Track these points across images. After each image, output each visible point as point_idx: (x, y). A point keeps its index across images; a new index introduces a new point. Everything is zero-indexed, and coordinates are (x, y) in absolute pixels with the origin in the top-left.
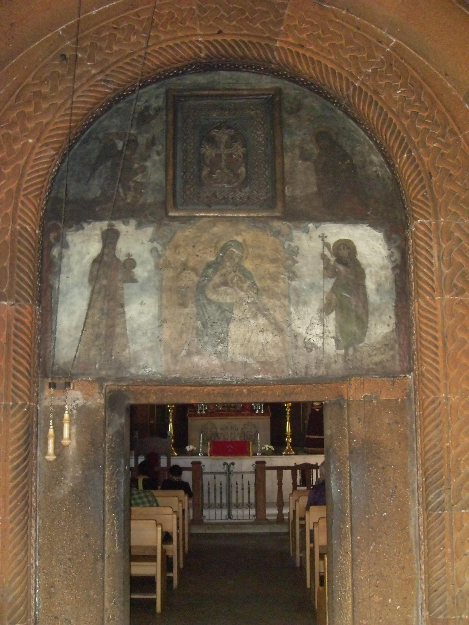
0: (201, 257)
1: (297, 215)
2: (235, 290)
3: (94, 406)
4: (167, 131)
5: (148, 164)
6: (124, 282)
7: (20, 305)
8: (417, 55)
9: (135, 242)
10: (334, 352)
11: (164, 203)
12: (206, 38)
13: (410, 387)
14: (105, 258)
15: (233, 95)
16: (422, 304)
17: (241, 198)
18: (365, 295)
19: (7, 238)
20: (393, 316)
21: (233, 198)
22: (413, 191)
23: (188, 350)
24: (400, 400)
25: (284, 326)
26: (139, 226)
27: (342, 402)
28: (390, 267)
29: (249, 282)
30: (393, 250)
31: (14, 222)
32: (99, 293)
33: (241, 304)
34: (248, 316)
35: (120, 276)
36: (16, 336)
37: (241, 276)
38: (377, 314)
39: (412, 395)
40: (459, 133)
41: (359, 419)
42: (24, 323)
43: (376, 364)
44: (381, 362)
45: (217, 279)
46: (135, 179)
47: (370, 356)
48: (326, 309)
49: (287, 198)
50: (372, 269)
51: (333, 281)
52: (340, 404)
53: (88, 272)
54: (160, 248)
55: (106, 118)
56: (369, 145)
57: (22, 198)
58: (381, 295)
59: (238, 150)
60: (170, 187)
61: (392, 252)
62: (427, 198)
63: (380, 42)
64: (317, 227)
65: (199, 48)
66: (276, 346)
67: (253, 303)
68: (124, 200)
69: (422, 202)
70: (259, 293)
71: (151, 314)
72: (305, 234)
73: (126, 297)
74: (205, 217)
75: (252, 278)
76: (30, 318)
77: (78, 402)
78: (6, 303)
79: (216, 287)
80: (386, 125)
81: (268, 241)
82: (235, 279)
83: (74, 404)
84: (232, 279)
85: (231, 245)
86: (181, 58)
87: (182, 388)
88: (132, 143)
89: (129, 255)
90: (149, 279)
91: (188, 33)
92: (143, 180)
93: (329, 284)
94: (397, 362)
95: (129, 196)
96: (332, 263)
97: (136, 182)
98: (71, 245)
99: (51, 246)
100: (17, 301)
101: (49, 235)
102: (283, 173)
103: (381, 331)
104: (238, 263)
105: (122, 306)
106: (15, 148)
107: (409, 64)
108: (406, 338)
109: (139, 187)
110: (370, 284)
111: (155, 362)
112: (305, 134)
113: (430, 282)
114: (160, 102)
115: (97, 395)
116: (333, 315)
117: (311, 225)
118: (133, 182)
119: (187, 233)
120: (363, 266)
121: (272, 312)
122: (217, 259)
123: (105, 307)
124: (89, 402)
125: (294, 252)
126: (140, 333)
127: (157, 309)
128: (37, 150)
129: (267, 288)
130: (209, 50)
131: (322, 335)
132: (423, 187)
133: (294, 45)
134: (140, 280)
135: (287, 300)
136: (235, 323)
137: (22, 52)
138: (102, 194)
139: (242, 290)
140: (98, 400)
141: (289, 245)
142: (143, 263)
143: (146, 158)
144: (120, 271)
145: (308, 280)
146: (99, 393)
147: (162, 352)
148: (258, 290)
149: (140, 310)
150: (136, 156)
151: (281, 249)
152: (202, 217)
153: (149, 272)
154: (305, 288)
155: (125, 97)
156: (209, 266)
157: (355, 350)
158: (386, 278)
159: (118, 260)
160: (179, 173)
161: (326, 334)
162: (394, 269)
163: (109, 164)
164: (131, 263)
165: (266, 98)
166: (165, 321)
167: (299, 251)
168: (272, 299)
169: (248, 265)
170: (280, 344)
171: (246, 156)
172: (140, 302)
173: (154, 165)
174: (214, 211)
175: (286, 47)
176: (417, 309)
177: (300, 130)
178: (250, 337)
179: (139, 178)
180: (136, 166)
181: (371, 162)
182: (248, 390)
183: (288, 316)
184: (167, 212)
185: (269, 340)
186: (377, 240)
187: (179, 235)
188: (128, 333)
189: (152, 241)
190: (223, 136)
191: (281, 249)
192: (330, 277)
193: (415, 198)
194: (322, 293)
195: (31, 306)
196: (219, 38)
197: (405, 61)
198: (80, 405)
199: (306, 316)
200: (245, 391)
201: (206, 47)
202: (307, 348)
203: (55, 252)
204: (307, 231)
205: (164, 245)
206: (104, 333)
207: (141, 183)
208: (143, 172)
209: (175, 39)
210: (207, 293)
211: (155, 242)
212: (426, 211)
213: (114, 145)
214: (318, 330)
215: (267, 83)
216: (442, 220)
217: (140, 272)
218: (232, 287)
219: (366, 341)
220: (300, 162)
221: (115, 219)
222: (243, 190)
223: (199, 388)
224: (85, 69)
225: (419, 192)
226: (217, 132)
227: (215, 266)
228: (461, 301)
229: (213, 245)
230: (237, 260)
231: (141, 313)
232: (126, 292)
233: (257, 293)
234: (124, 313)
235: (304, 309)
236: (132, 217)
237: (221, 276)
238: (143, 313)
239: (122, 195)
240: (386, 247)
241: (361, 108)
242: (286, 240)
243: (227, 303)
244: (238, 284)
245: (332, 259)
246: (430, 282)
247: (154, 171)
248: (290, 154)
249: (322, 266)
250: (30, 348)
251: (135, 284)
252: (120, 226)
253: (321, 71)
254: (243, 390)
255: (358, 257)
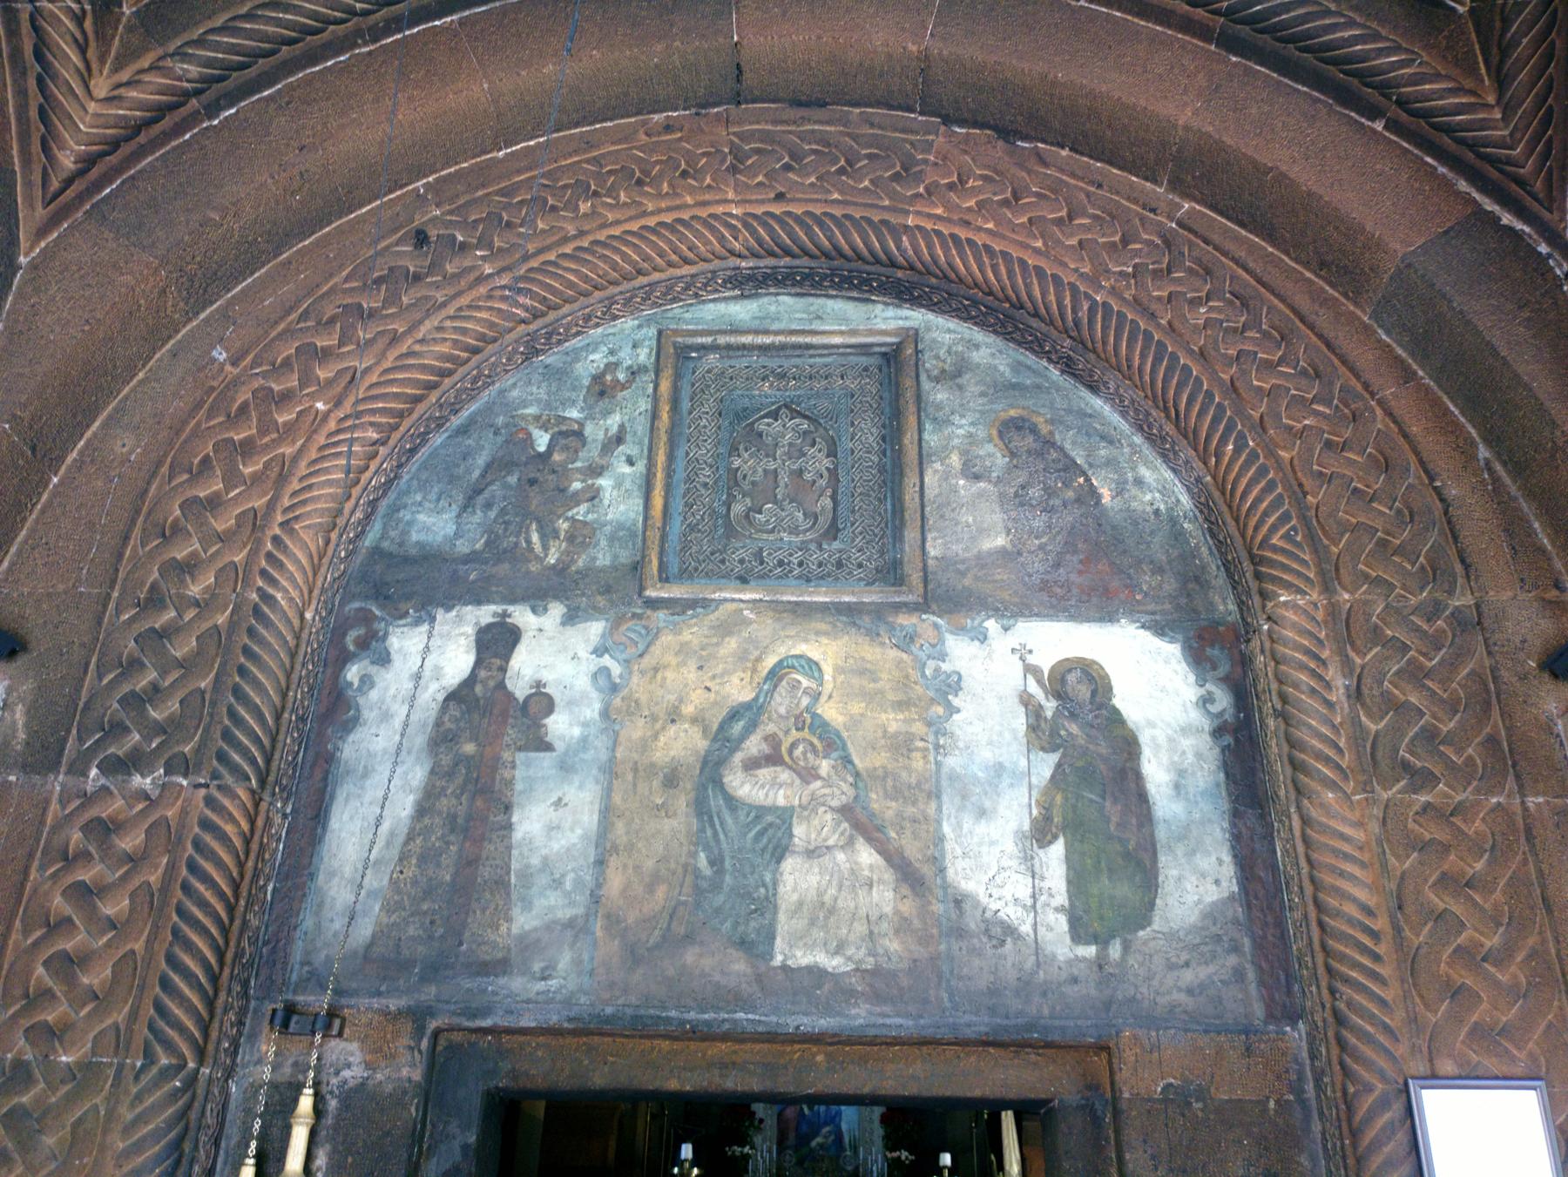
0: (717, 693)
1: (956, 598)
2: (799, 774)
3: (389, 1088)
4: (655, 415)
5: (604, 482)
6: (520, 749)
7: (219, 787)
8: (1243, 232)
9: (557, 656)
10: (1066, 950)
11: (637, 567)
12: (750, 209)
13: (1296, 1061)
14: (478, 689)
15: (808, 347)
16: (1314, 813)
17: (820, 565)
18: (1143, 797)
19: (221, 619)
20: (1227, 858)
21: (800, 564)
22: (1256, 528)
23: (669, 928)
24: (1272, 1104)
25: (927, 870)
26: (570, 619)
27: (1097, 1106)
28: (1207, 728)
29: (835, 755)
30: (1209, 686)
31: (247, 582)
32: (450, 775)
33: (815, 811)
34: (831, 842)
35: (511, 734)
36: (193, 867)
37: (815, 741)
38: (1180, 850)
39: (1310, 1087)
40: (1367, 396)
41: (1153, 1157)
42: (223, 838)
43: (1190, 991)
44: (1203, 987)
45: (754, 745)
46: (570, 514)
47: (1171, 967)
48: (1041, 833)
49: (930, 562)
50: (1157, 732)
51: (1053, 758)
52: (1093, 1111)
53: (431, 721)
54: (616, 670)
55: (514, 385)
56: (1131, 445)
57: (277, 531)
58: (1187, 800)
59: (817, 461)
60: (654, 536)
61: (1209, 693)
62: (1298, 545)
63: (1153, 210)
64: (1006, 629)
65: (735, 227)
66: (902, 926)
67: (845, 811)
68: (540, 560)
69: (1283, 551)
70: (860, 784)
71: (579, 832)
72: (976, 643)
73: (519, 786)
74: (733, 600)
75: (844, 747)
76: (245, 826)
77: (346, 1073)
78: (185, 783)
79: (752, 765)
80: (1175, 381)
81: (883, 656)
82: (801, 748)
83: (334, 1081)
84: (793, 746)
85: (793, 667)
86: (690, 249)
87: (648, 1043)
88: (570, 437)
89: (539, 684)
90: (584, 741)
91: (707, 197)
92: (590, 517)
93: (1045, 766)
94: (1253, 988)
95: (553, 550)
96: (1049, 714)
97: (573, 520)
98: (394, 656)
99: (345, 658)
100: (215, 776)
101: (345, 634)
102: (923, 507)
103: (1196, 898)
104: (807, 709)
105: (508, 808)
106: (280, 420)
107: (1225, 254)
108: (1270, 919)
109: (581, 536)
110: (1156, 772)
111: (577, 962)
112: (972, 424)
113: (1331, 753)
114: (644, 356)
115: (405, 1057)
116: (1058, 849)
117: (992, 625)
118: (567, 519)
119: (686, 636)
120: (1131, 725)
121: (893, 835)
122: (756, 699)
123: (462, 811)
124: (379, 1076)
125: (949, 686)
126: (543, 880)
127: (596, 817)
128: (332, 425)
129: (880, 772)
130: (753, 232)
131: (1029, 902)
132: (1286, 518)
133: (949, 220)
134: (560, 746)
135: (933, 805)
136: (799, 860)
137: (329, 224)
138: (487, 544)
139: (818, 777)
140: (411, 1071)
141: (937, 670)
142: (571, 703)
143: (596, 471)
144: (511, 720)
145: (987, 755)
146: (411, 1049)
147: (599, 933)
148: (857, 775)
149: (551, 821)
150: (579, 464)
151: (914, 675)
152: (725, 600)
153: (585, 725)
154: (980, 774)
155: (559, 342)
156: (734, 715)
157: (1126, 947)
158: (1199, 755)
159: (510, 696)
160: (678, 505)
161: (1043, 898)
162: (1217, 732)
163: (512, 479)
164: (542, 701)
165: (885, 354)
166: (615, 849)
167: (963, 684)
168: (895, 799)
169: (830, 712)
170: (917, 923)
171: (833, 473)
172: (554, 799)
173: (618, 485)
174: (752, 590)
175: (929, 226)
176: (1297, 833)
177: (963, 416)
178: (836, 899)
179: (580, 512)
180: (577, 485)
181: (1139, 482)
182: (829, 1056)
183: (936, 845)
184: (642, 589)
185: (888, 909)
186: (1167, 662)
187: (666, 639)
188: (513, 880)
189: (599, 651)
190: (785, 431)
191: (914, 675)
192: (1043, 749)
193: (1264, 543)
194: (1026, 790)
195: (253, 792)
196: (777, 209)
197: (1216, 248)
198: (352, 1083)
199: (984, 849)
200: (819, 1058)
201: (746, 225)
202: (990, 937)
203: (353, 673)
204: (983, 638)
205: (627, 662)
206: (448, 878)
207: (585, 523)
208: (593, 499)
209: (678, 208)
210: (725, 780)
211: (607, 656)
212: (1299, 574)
213: (529, 440)
214: (1021, 887)
215: (886, 319)
216: (1347, 596)
217: (559, 725)
218: (790, 768)
219: (1157, 924)
220: (961, 482)
221: (513, 601)
222: (825, 546)
223: (693, 1045)
224: (467, 263)
225: (1274, 528)
226: (769, 425)
227: (749, 713)
228: (1427, 807)
229: (749, 665)
230: (805, 701)
231: (552, 829)
232: (519, 773)
233: (855, 785)
234: (509, 827)
235: (982, 828)
236: (556, 598)
237: (766, 739)
238: (558, 827)
239: (538, 547)
240: (1192, 678)
241: (1110, 348)
242: (929, 657)
243: (778, 808)
244: (806, 759)
245: (1050, 706)
246: (1331, 753)
247: (618, 498)
248: (938, 466)
249: (1020, 722)
250: (231, 909)
251: (548, 754)
252: (522, 616)
253: (1010, 273)
254: (814, 1056)
255: (1117, 702)
